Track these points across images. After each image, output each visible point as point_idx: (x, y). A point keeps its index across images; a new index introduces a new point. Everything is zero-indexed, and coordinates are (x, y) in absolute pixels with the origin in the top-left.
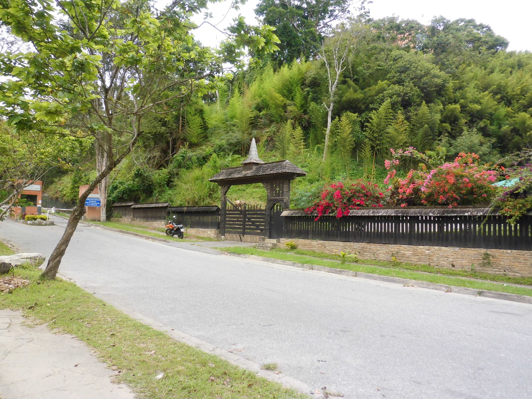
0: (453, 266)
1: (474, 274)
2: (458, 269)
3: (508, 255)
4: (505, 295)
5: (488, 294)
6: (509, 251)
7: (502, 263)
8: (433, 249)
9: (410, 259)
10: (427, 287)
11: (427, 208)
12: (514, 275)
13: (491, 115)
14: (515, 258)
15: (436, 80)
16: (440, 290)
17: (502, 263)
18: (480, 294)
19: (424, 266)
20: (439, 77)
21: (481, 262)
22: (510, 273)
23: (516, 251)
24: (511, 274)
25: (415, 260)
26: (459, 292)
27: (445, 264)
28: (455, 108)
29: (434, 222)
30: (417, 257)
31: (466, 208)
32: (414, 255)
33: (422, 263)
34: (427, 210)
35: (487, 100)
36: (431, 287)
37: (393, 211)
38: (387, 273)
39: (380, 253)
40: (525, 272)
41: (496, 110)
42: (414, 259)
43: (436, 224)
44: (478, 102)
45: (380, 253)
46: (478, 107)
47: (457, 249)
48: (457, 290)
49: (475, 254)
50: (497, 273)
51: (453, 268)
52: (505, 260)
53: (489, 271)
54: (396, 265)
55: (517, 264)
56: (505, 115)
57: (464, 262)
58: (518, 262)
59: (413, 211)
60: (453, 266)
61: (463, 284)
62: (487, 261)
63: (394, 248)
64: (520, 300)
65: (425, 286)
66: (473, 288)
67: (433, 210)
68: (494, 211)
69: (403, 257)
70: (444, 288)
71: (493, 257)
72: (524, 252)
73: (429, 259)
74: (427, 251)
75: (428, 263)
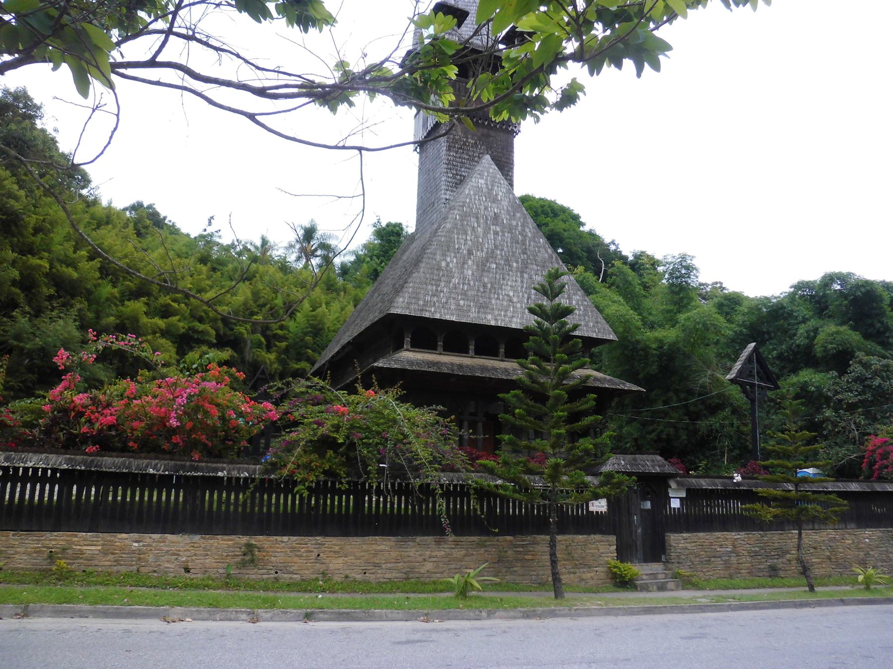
0: (187, 570)
1: (228, 583)
2: (196, 576)
3: (283, 544)
4: (348, 613)
5: (321, 615)
6: (285, 539)
7: (273, 559)
8: (148, 540)
9: (96, 562)
10: (211, 618)
11: (140, 458)
12: (291, 578)
13: (89, 292)
14: (293, 549)
15: (12, 202)
16: (237, 619)
17: (273, 559)
18: (308, 617)
19: (128, 575)
20: (17, 199)
21: (239, 559)
22: (285, 576)
23: (295, 538)
24: (285, 577)
25: (107, 563)
26: (272, 619)
27: (170, 566)
28: (40, 266)
29: (53, 481)
30: (111, 557)
31: (215, 462)
32: (105, 553)
33: (123, 569)
34: (140, 462)
35: (90, 269)
36: (218, 616)
37: (61, 458)
38: (105, 600)
39: (16, 553)
40: (307, 572)
41: (96, 286)
42: (105, 562)
43: (57, 487)
44: (73, 264)
45: (16, 553)
46: (75, 275)
47: (197, 538)
48: (269, 615)
49: (229, 547)
50: (265, 577)
51: (187, 575)
52: (277, 554)
53: (253, 574)
54: (64, 577)
55: (296, 559)
56: (108, 299)
57: (209, 561)
58: (297, 556)
59: (110, 463)
60: (187, 570)
61: (273, 605)
62: (250, 557)
63: (56, 540)
64: (370, 618)
65: (206, 615)
66: (295, 608)
67: (154, 462)
68: (267, 471)
69: (77, 558)
70: (244, 616)
71: (260, 549)
72: (307, 539)
73: (140, 559)
74: (136, 544)
75: (135, 568)
